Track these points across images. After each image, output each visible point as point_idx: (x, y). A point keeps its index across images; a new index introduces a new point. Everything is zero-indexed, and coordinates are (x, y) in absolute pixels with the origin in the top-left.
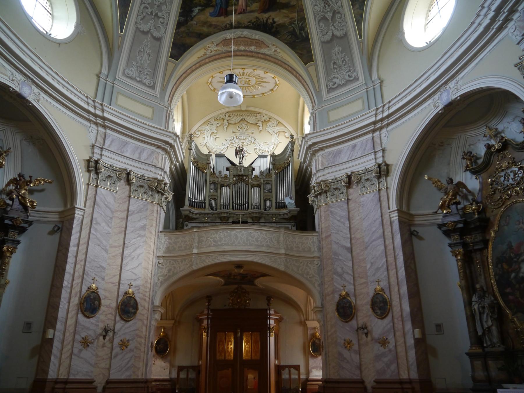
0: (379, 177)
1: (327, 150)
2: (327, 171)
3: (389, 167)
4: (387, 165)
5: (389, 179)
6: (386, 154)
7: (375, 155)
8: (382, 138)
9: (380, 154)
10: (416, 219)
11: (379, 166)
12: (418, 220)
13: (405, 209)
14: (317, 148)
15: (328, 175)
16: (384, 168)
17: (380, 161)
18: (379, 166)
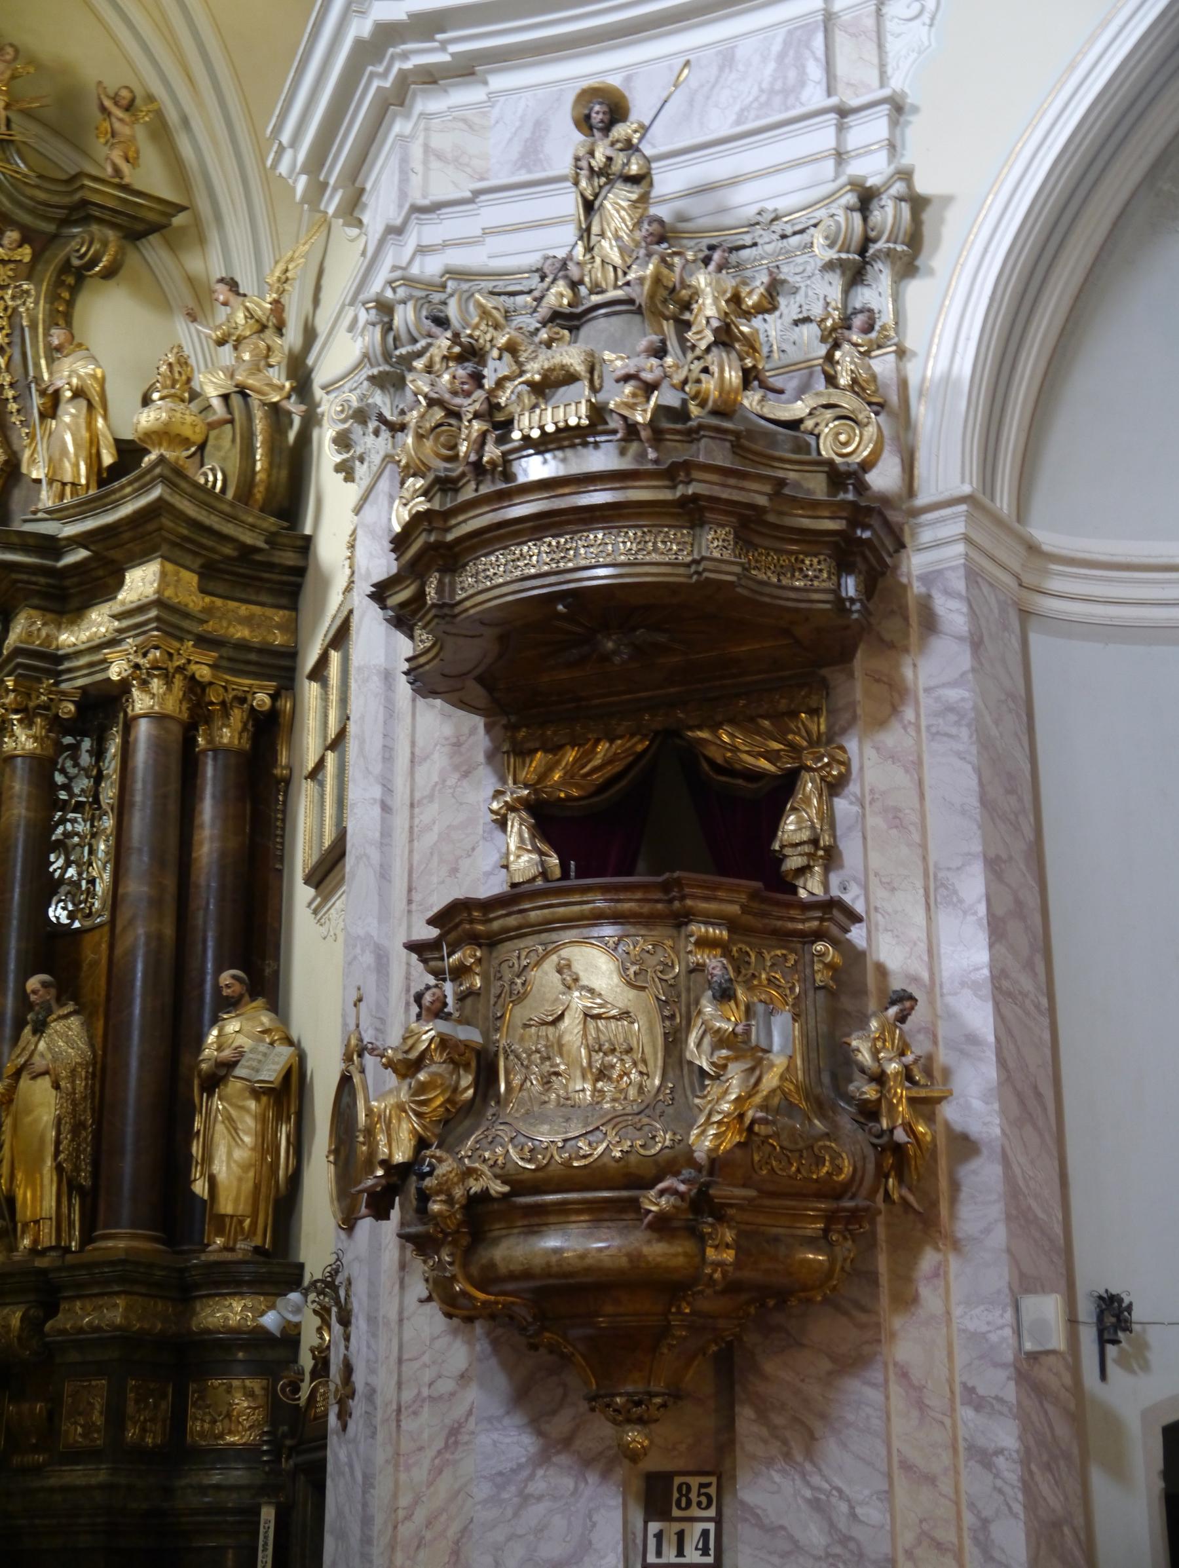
0: (855, 274)
1: (499, 81)
2: (492, 213)
3: (927, 216)
4: (918, 203)
5: (914, 289)
6: (915, 131)
7: (841, 129)
8: (890, 26)
9: (870, 130)
10: (1055, 585)
11: (866, 199)
12: (1067, 595)
13: (1004, 503)
14: (443, 58)
15: (496, 244)
16: (886, 214)
17: (873, 168)
18: (866, 199)
